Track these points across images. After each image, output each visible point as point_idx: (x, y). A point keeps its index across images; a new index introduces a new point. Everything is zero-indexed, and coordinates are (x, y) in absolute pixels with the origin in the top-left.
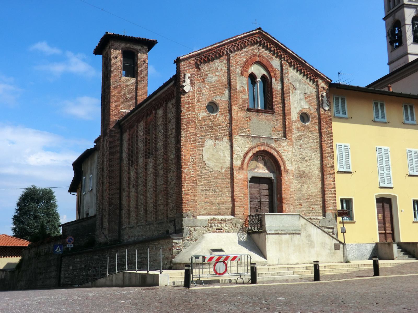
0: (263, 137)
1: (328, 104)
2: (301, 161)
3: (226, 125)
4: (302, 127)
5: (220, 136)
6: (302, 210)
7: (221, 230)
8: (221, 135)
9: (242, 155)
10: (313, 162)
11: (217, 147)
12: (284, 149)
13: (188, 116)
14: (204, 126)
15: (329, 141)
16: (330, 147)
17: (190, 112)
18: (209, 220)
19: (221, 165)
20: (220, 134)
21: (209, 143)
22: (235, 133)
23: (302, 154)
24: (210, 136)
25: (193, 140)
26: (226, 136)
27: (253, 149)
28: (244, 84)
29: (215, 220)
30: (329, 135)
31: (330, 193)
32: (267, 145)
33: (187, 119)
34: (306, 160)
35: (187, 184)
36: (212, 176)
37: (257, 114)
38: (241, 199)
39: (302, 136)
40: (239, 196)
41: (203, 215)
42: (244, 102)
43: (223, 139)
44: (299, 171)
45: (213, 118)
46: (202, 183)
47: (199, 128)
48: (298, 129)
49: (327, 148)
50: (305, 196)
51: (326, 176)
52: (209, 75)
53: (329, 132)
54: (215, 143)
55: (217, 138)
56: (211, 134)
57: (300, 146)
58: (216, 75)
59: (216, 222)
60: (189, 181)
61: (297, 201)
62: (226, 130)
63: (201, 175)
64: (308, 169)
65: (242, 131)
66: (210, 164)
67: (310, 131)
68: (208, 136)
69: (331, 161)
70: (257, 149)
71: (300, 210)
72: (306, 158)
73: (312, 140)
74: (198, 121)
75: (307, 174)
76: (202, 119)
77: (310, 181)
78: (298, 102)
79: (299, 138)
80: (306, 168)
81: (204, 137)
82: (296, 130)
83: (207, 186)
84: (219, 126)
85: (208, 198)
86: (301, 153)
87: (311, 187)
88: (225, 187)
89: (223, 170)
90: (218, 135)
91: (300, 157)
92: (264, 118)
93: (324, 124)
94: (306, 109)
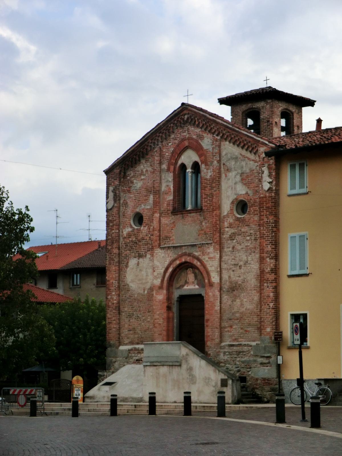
0: (185, 246)
1: (271, 180)
2: (234, 269)
3: (150, 237)
4: (236, 222)
5: (144, 252)
6: (232, 334)
7: (141, 360)
8: (144, 250)
9: (162, 271)
10: (249, 268)
11: (140, 265)
12: (209, 256)
13: (112, 235)
14: (129, 243)
15: (270, 234)
16: (270, 243)
17: (113, 231)
18: (129, 350)
19: (144, 286)
20: (143, 249)
21: (133, 262)
22: (155, 246)
23: (234, 259)
24: (134, 253)
25: (116, 262)
26: (149, 251)
27: (174, 263)
28: (169, 181)
29: (135, 349)
30: (270, 226)
31: (267, 309)
32: (189, 255)
33: (111, 239)
34: (240, 267)
35: (110, 311)
36: (135, 300)
37: (183, 217)
38: (160, 324)
39: (236, 233)
40: (158, 320)
41: (126, 344)
42: (168, 205)
43: (146, 255)
44: (231, 282)
45: (137, 233)
46: (126, 309)
47: (124, 246)
48: (231, 226)
49: (266, 245)
50: (237, 315)
51: (263, 285)
52: (135, 181)
53: (270, 221)
54: (139, 262)
55: (141, 255)
56: (135, 251)
57: (233, 248)
58: (142, 179)
59: (136, 352)
60: (112, 307)
61: (227, 322)
62: (149, 243)
63: (125, 300)
64: (242, 278)
65: (166, 242)
66: (133, 286)
67: (246, 226)
68: (132, 255)
69: (271, 263)
70: (178, 262)
71: (230, 333)
72: (239, 264)
73: (248, 238)
74: (124, 238)
75: (239, 286)
76: (127, 236)
77: (245, 294)
78: (232, 188)
79: (232, 237)
80: (239, 277)
81: (128, 256)
82: (228, 227)
83: (130, 311)
84: (143, 240)
85: (131, 325)
86: (233, 257)
87: (246, 302)
88: (148, 311)
89: (146, 292)
90: (141, 251)
91: (231, 263)
92: (190, 219)
93: (264, 212)
94: (243, 194)
